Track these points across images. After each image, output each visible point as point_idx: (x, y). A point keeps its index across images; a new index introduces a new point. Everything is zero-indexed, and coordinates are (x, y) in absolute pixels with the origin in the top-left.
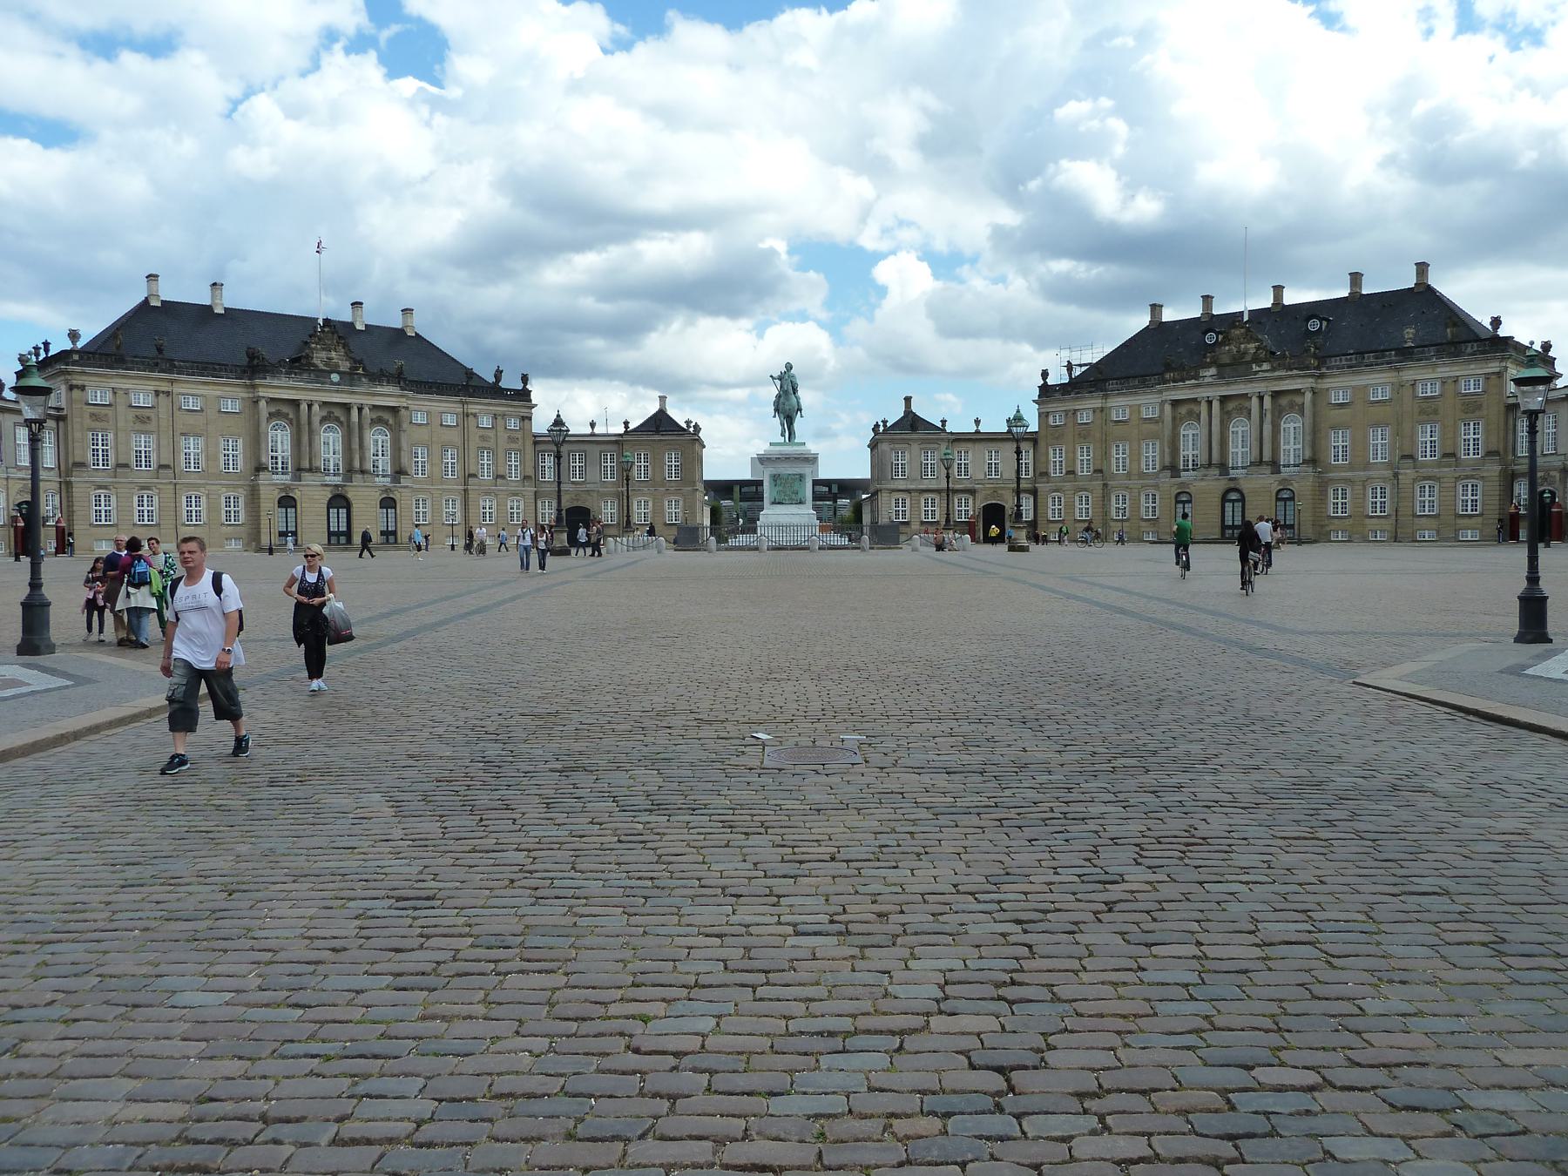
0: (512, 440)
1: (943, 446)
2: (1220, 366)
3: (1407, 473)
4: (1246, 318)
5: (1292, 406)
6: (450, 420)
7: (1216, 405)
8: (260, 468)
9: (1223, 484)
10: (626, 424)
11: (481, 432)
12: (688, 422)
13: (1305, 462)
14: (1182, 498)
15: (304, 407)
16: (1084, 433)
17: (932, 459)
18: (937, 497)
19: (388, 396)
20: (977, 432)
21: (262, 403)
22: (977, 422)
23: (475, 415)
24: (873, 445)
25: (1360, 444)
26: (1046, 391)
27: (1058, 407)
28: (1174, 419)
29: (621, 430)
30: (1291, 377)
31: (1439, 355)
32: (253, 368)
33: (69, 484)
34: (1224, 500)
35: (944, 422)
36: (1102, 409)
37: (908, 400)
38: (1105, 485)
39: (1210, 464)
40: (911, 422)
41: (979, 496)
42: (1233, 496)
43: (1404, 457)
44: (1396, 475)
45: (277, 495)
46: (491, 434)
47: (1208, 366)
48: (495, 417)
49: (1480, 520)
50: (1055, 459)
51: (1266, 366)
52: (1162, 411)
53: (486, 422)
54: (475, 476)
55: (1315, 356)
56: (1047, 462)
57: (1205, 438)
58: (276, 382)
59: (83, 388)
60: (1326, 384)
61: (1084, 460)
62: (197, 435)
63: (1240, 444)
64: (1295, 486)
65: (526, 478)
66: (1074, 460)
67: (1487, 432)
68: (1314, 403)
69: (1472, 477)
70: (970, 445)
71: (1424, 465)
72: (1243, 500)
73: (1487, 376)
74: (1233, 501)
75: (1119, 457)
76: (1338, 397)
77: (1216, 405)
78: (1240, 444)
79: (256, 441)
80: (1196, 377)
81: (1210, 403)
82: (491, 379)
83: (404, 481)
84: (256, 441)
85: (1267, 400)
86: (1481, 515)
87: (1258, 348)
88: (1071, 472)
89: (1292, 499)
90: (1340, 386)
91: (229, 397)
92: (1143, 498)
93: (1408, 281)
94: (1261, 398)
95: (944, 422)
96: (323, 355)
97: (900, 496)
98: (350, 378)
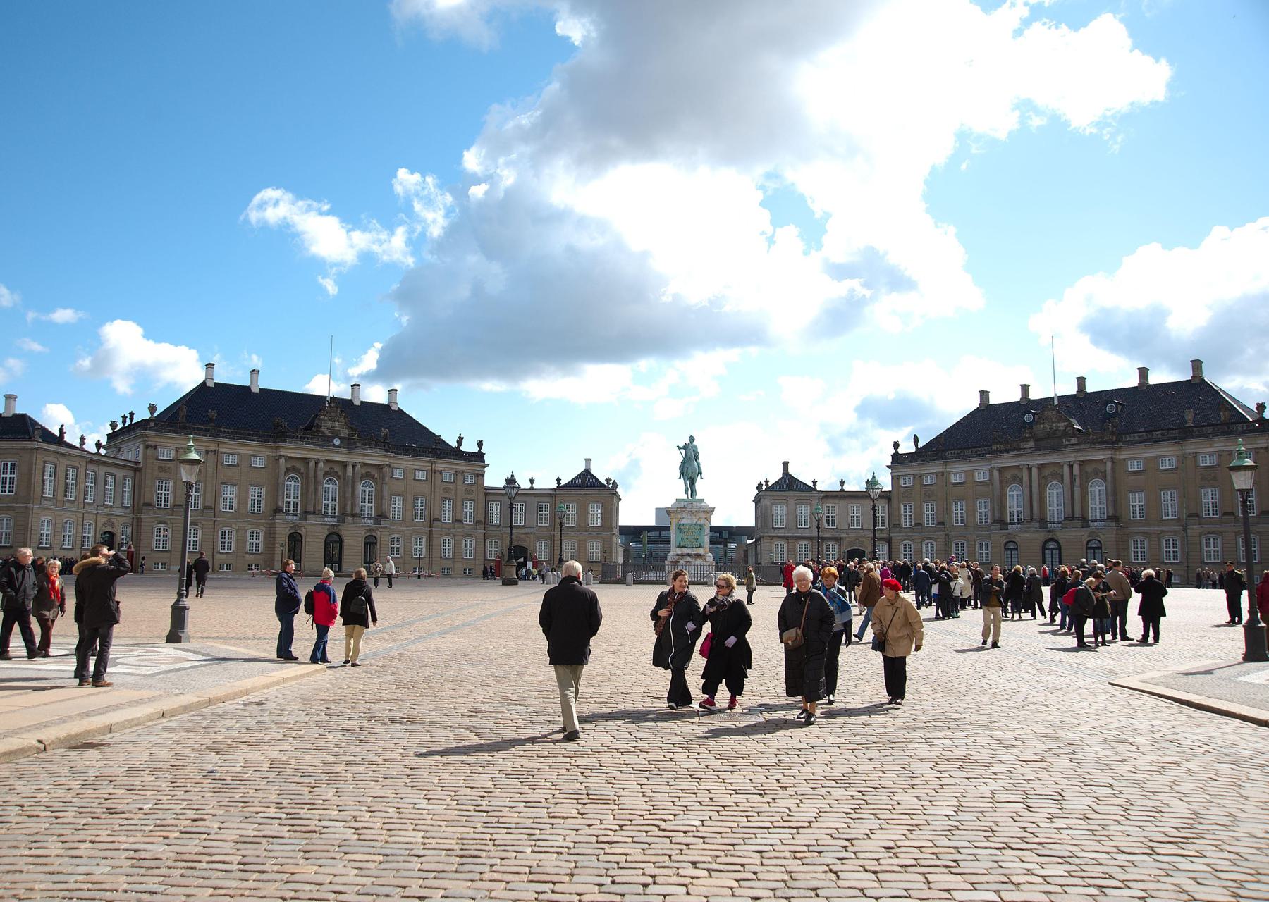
0: (468, 492)
1: (815, 501)
2: (1036, 440)
3: (1194, 529)
4: (1056, 403)
6: (421, 475)
7: (1035, 471)
8: (277, 511)
9: (1042, 536)
10: (559, 480)
11: (445, 486)
12: (608, 480)
13: (1109, 517)
14: (1011, 547)
15: (312, 464)
16: (929, 493)
17: (804, 511)
19: (375, 457)
20: (842, 491)
21: (282, 461)
22: (842, 483)
23: (441, 472)
24: (757, 501)
25: (1153, 504)
26: (898, 459)
27: (907, 471)
28: (1001, 482)
29: (555, 486)
31: (1216, 434)
32: (275, 434)
33: (139, 520)
34: (1044, 548)
35: (815, 483)
36: (943, 474)
37: (786, 464)
38: (947, 535)
39: (1032, 519)
40: (788, 482)
42: (1052, 545)
43: (1190, 515)
44: (1185, 530)
45: (288, 531)
46: (452, 487)
47: (1028, 440)
48: (456, 473)
50: (906, 513)
51: (1074, 441)
52: (991, 475)
53: (448, 478)
54: (438, 520)
55: (1113, 433)
56: (900, 515)
57: (1027, 498)
58: (293, 445)
59: (155, 447)
60: (1124, 454)
61: (929, 514)
62: (233, 484)
63: (1055, 501)
64: (1102, 538)
65: (478, 522)
66: (921, 513)
68: (1113, 469)
71: (1211, 521)
72: (1059, 548)
74: (1052, 549)
75: (957, 511)
76: (1133, 466)
77: (1035, 471)
78: (1055, 501)
79: (275, 490)
80: (1018, 449)
81: (1030, 470)
82: (454, 444)
83: (384, 523)
84: (275, 490)
85: (1076, 467)
87: (1066, 427)
88: (919, 524)
89: (1100, 548)
90: (1134, 458)
91: (258, 455)
92: (978, 546)
93: (1185, 375)
94: (1071, 466)
95: (815, 483)
96: (329, 424)
97: (779, 542)
98: (348, 443)
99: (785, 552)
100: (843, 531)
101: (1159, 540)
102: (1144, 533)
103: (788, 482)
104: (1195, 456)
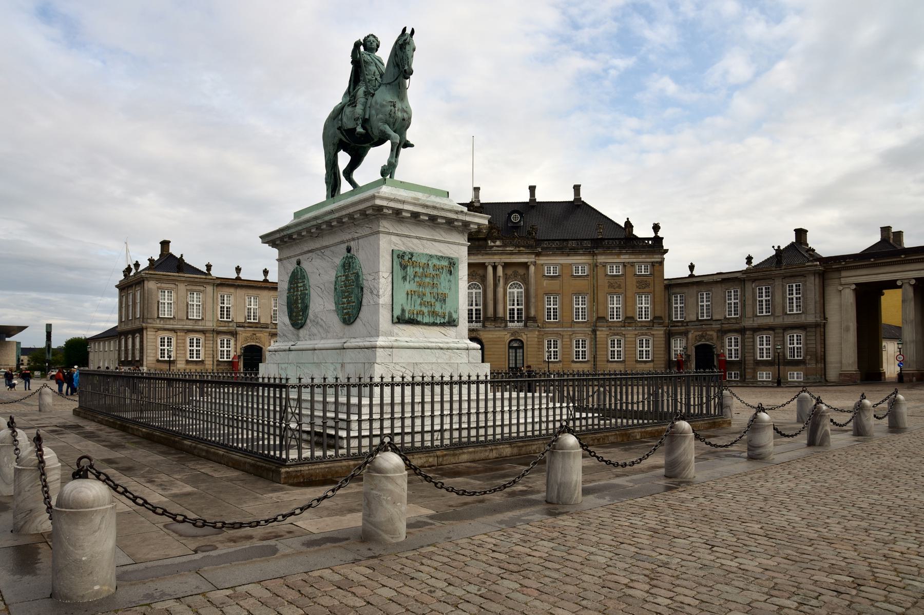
5: (516, 275)
18: (201, 337)
20: (238, 278)
22: (238, 270)
30: (519, 253)
31: (621, 247)
35: (209, 267)
40: (169, 264)
41: (241, 337)
44: (594, 331)
49: (652, 364)
60: (542, 260)
64: (524, 338)
67: (654, 303)
69: (646, 334)
70: (232, 290)
73: (653, 264)
85: (500, 270)
86: (652, 361)
90: (551, 264)
93: (571, 198)
94: (495, 268)
95: (209, 267)
99: (173, 348)
100: (240, 325)
101: (571, 341)
102: (558, 334)
103: (169, 264)
104: (604, 265)
